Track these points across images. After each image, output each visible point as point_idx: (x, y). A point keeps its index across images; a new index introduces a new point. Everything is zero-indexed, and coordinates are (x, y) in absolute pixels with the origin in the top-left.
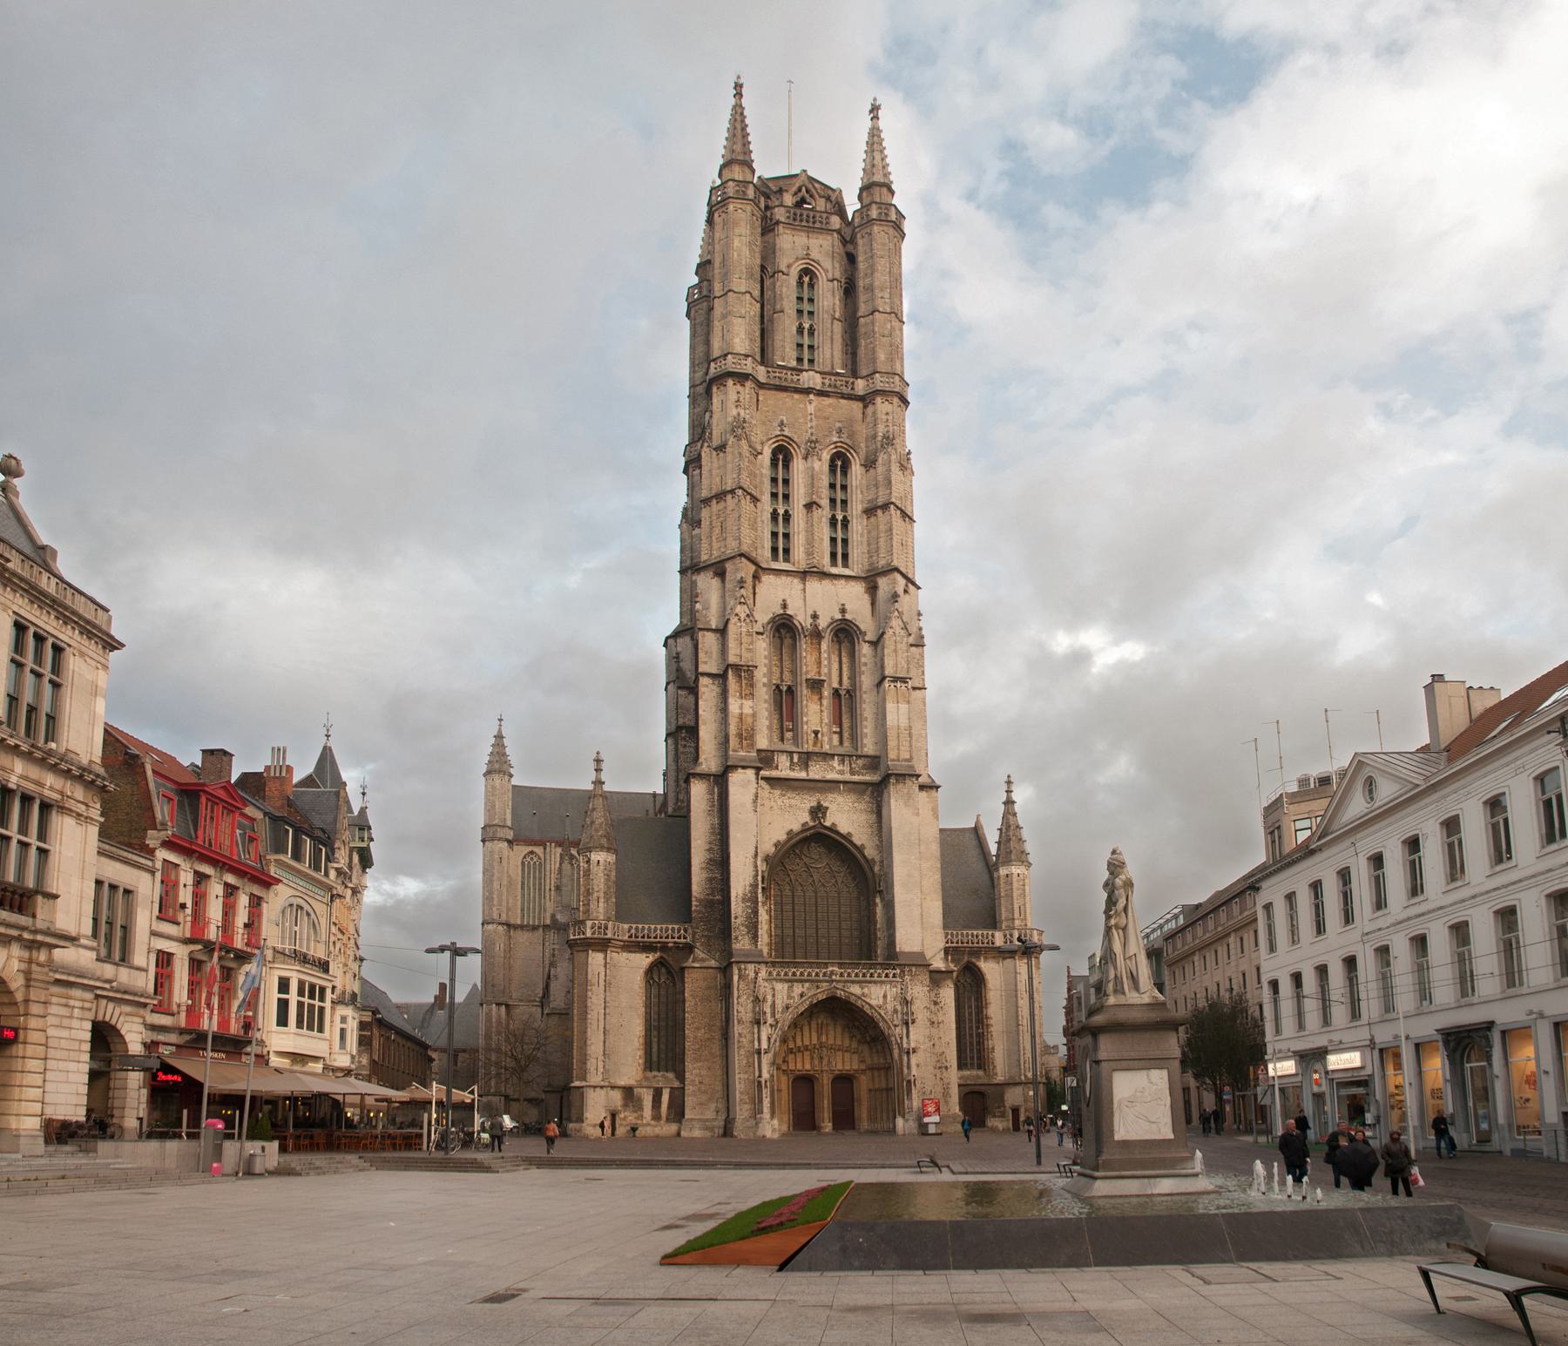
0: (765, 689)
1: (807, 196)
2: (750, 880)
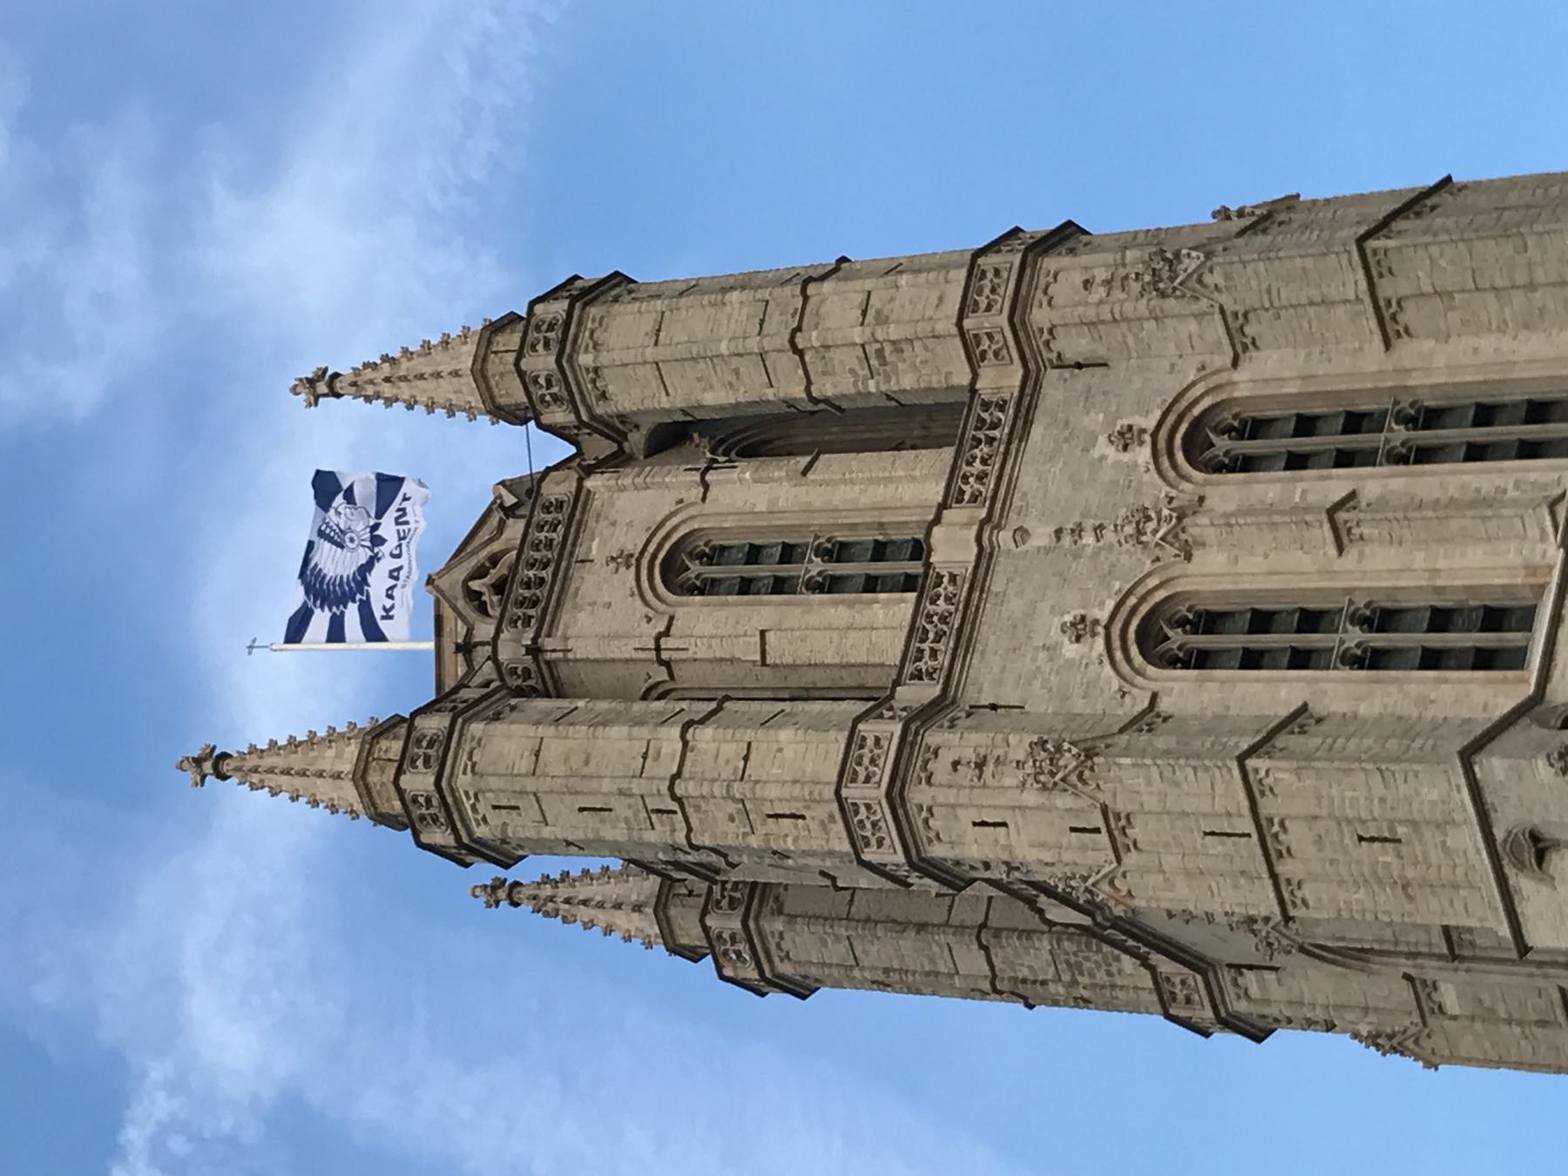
1: (494, 574)
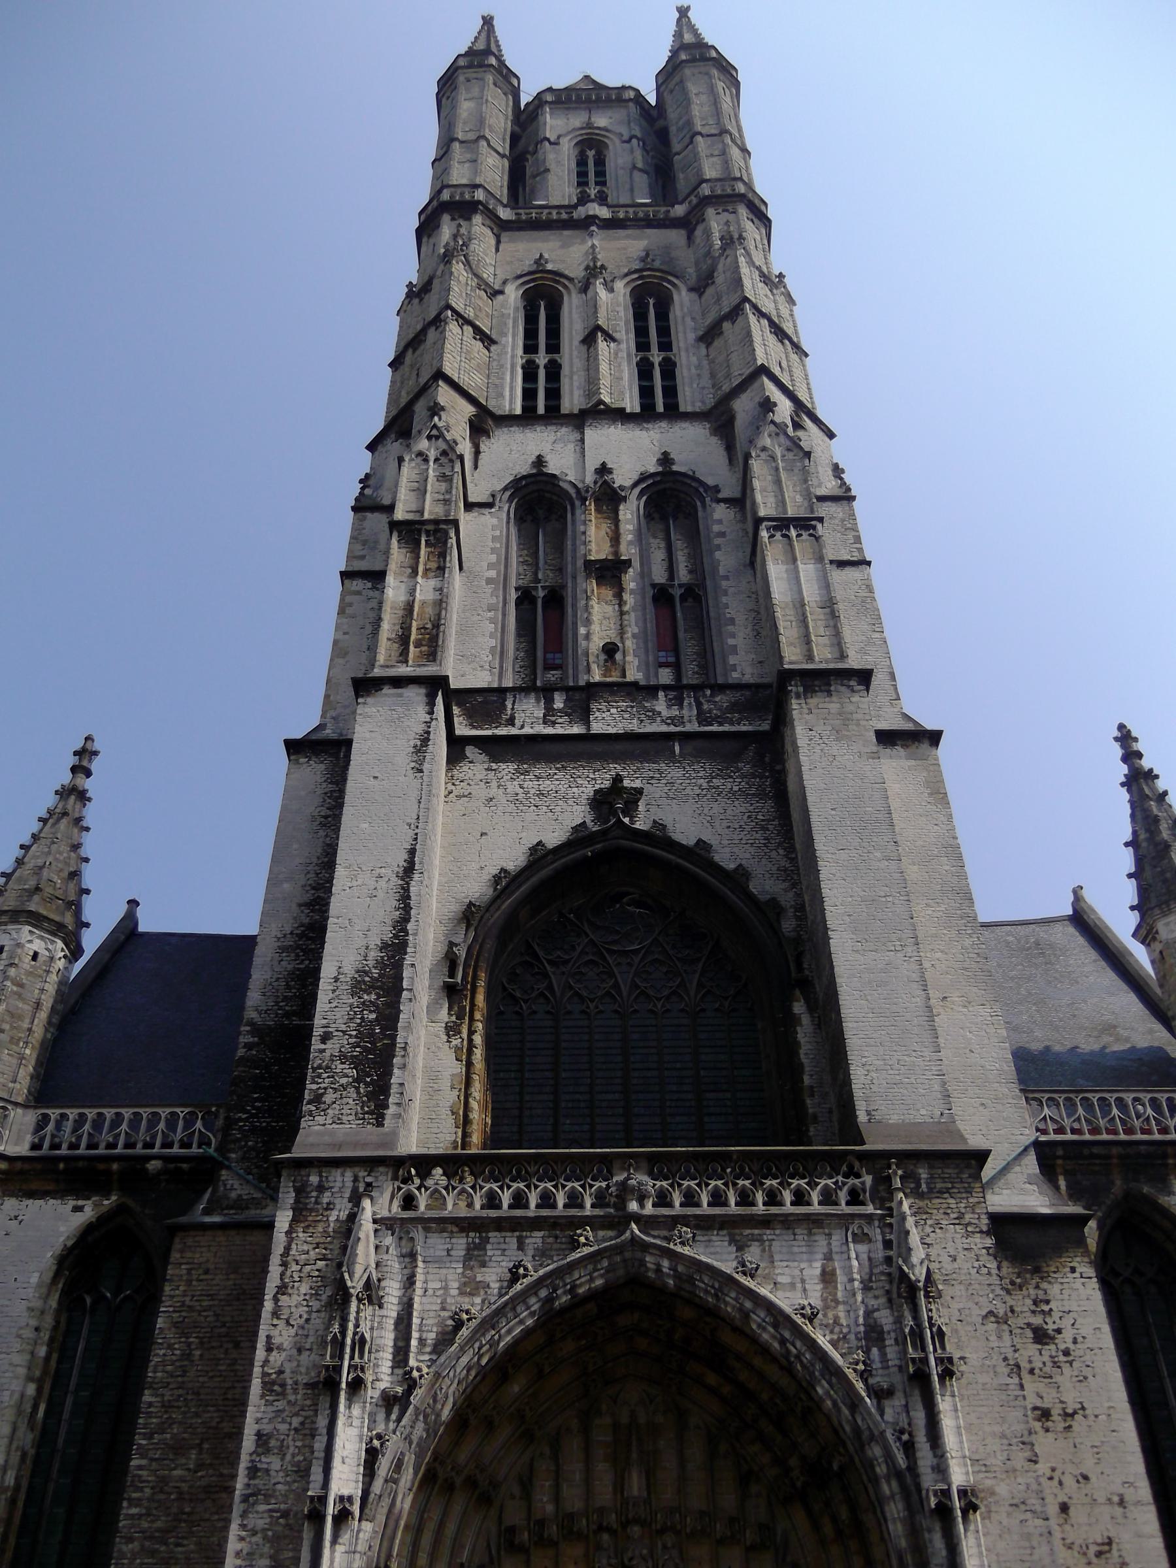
0: (489, 589)
2: (382, 932)
